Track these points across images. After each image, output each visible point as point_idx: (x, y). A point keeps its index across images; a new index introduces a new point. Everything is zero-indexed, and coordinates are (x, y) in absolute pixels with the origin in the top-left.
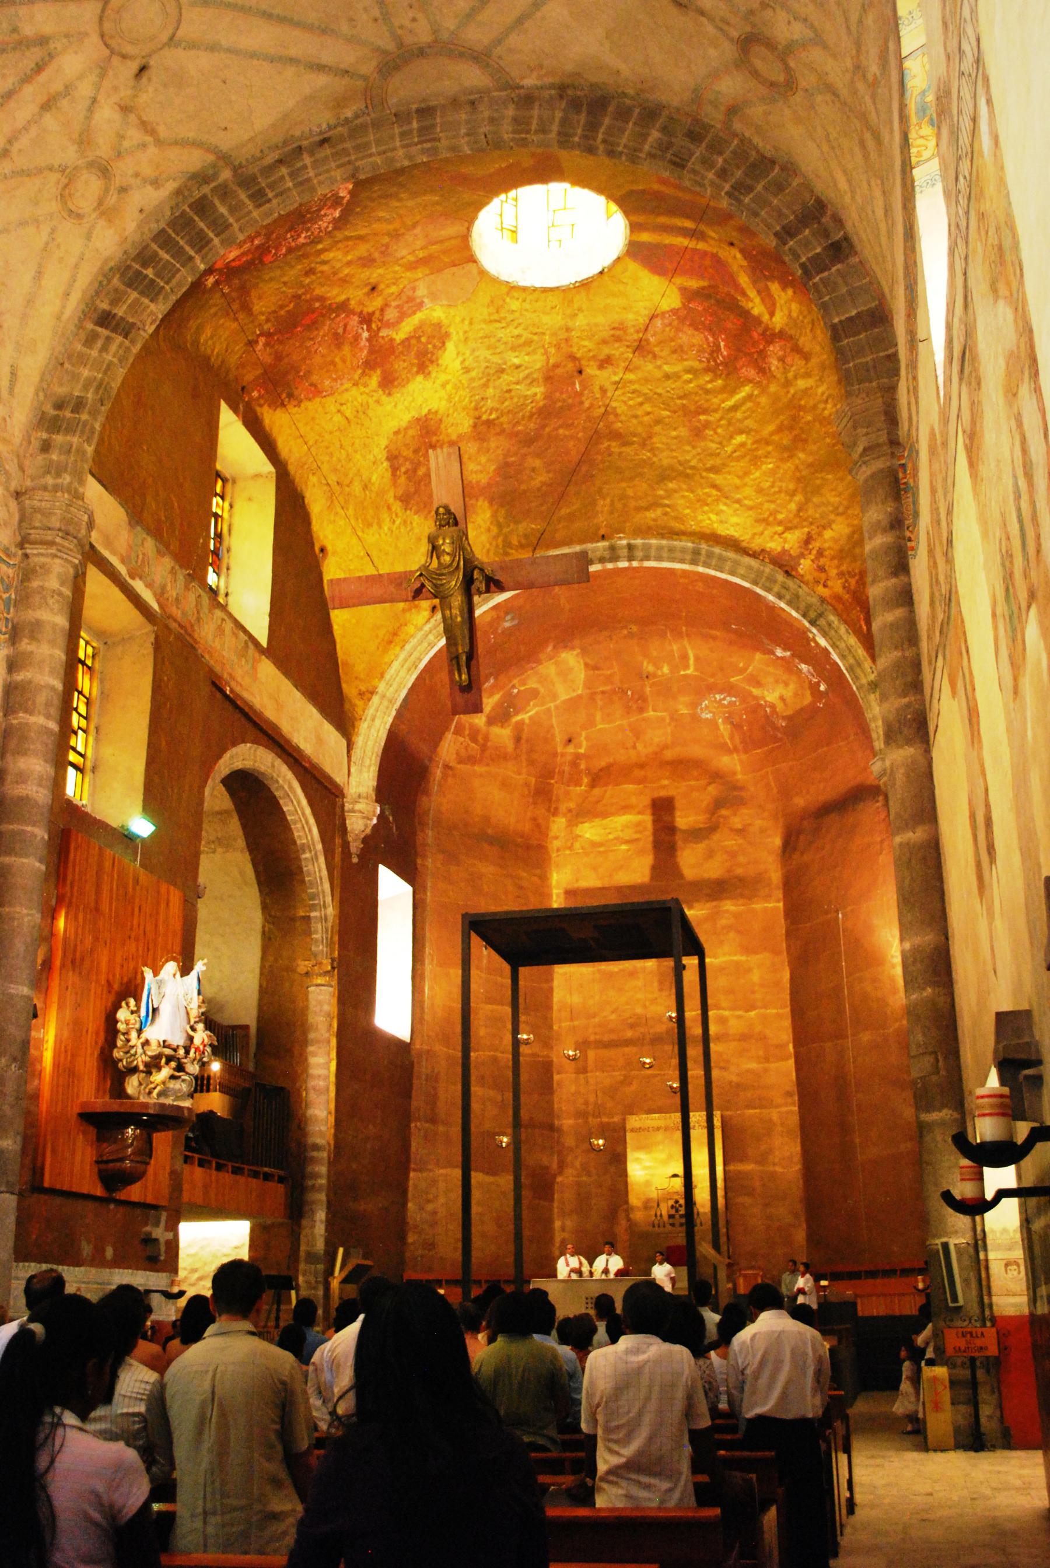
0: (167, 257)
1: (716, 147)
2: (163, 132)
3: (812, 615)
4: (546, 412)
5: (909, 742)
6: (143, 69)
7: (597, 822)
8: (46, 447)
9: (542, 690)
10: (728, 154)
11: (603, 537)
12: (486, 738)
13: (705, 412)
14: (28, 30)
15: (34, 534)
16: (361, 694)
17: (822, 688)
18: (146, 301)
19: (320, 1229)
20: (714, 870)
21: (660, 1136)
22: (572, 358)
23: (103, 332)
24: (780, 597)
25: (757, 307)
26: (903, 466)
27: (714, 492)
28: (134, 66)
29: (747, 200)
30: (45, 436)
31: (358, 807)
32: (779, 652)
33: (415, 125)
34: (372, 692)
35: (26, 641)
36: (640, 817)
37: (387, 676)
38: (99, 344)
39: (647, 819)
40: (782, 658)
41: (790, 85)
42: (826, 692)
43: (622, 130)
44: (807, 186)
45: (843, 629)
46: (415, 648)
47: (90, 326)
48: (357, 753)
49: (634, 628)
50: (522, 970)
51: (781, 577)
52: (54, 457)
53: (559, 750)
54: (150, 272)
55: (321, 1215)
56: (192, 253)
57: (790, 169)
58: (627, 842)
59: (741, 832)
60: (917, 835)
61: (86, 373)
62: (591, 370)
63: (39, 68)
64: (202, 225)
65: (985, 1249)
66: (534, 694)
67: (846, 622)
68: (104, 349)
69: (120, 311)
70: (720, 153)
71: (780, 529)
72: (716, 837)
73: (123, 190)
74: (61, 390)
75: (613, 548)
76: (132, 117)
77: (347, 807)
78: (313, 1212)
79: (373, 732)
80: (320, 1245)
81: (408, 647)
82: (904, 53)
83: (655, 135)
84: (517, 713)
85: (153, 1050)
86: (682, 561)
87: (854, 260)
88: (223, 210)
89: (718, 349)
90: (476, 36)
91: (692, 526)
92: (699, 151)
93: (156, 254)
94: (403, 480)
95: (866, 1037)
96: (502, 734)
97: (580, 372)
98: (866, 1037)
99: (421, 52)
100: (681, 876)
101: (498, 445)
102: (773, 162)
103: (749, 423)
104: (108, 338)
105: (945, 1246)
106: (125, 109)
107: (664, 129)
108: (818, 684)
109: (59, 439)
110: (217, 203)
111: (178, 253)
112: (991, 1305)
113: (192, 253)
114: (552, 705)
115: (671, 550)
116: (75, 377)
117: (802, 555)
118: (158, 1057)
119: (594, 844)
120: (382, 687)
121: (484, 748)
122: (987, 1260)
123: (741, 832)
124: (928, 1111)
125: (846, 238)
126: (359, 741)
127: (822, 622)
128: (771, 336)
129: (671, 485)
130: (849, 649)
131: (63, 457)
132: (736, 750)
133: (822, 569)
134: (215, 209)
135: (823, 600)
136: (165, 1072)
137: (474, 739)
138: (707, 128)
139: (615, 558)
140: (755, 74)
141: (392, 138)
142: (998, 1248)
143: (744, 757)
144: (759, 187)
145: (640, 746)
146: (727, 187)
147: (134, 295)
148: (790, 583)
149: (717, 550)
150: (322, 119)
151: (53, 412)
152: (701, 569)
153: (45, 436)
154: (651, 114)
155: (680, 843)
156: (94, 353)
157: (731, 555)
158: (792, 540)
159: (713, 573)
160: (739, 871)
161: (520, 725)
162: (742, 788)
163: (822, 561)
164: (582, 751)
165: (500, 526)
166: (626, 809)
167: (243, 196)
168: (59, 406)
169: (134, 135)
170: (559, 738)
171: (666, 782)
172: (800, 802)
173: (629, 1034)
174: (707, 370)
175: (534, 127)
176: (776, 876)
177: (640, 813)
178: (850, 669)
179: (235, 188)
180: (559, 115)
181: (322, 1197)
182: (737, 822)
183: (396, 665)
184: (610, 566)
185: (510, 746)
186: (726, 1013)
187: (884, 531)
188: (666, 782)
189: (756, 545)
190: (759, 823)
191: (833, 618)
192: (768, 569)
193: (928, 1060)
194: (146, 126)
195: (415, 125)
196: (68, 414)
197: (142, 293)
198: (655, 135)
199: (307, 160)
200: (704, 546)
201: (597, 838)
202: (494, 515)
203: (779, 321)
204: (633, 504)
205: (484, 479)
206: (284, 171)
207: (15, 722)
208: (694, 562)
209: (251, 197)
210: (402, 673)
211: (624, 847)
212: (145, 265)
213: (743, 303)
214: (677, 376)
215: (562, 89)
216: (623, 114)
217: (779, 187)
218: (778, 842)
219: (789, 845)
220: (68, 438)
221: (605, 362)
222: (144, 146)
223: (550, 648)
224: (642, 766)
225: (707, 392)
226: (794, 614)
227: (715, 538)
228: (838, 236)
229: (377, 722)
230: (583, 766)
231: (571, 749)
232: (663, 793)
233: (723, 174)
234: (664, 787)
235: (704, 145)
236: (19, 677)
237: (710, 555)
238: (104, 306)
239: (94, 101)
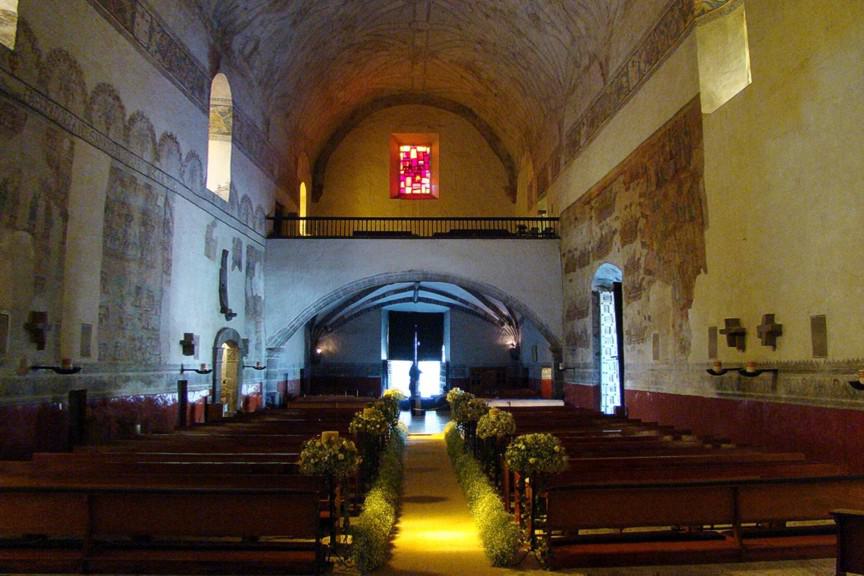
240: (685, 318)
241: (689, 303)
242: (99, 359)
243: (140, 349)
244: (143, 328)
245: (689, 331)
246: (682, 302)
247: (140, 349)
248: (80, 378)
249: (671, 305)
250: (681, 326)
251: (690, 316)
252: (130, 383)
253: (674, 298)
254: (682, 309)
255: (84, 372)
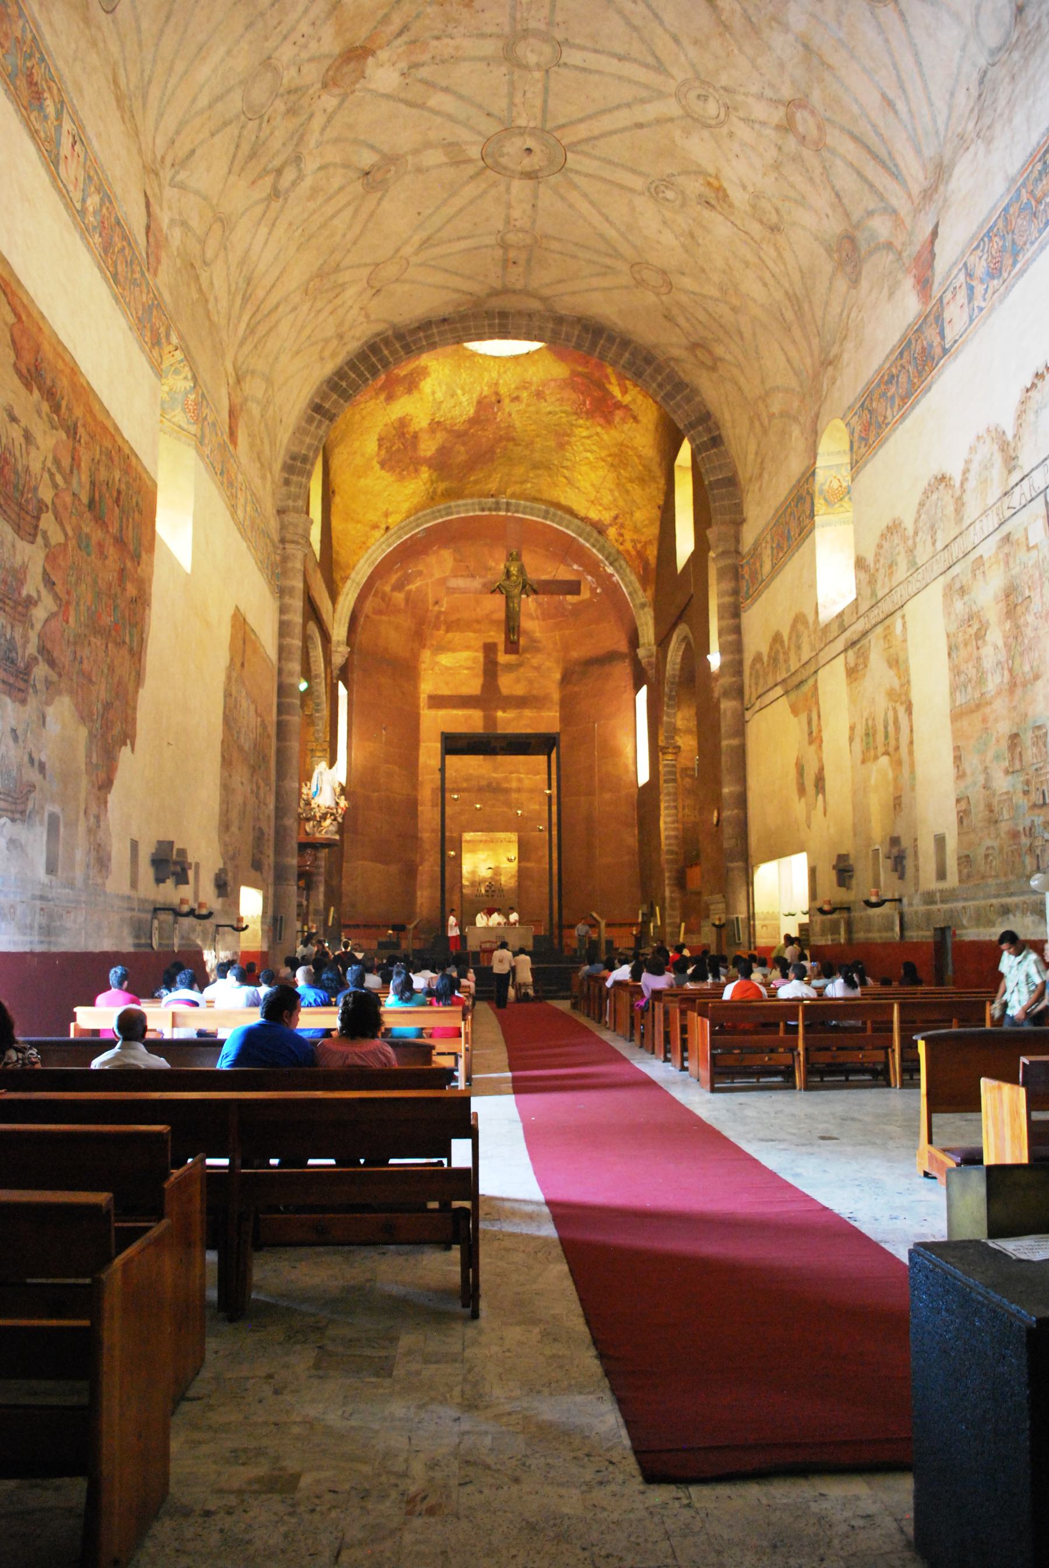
0: (353, 376)
1: (658, 370)
2: (373, 317)
3: (611, 559)
4: (474, 421)
5: (734, 699)
6: (378, 291)
7: (450, 654)
8: (287, 482)
9: (425, 571)
10: (664, 374)
11: (492, 496)
12: (390, 599)
13: (569, 435)
14: (340, 281)
15: (289, 536)
16: (342, 578)
17: (598, 591)
18: (342, 401)
19: (321, 897)
20: (519, 690)
21: (481, 845)
22: (497, 394)
23: (318, 417)
24: (594, 546)
25: (616, 391)
26: (742, 566)
27: (564, 480)
28: (374, 291)
29: (672, 403)
30: (286, 476)
31: (339, 649)
32: (575, 567)
33: (497, 321)
34: (347, 578)
35: (287, 598)
36: (476, 654)
37: (357, 568)
38: (315, 424)
39: (480, 656)
40: (577, 570)
41: (714, 369)
42: (599, 594)
43: (610, 348)
44: (702, 403)
45: (628, 570)
46: (374, 552)
47: (309, 411)
48: (337, 615)
49: (489, 541)
50: (448, 757)
51: (595, 534)
52: (292, 489)
53: (430, 608)
54: (344, 384)
55: (322, 889)
56: (368, 376)
57: (695, 391)
58: (467, 668)
59: (537, 669)
60: (735, 742)
61: (308, 440)
62: (506, 401)
63: (337, 296)
64: (374, 359)
65: (754, 920)
66: (420, 573)
67: (630, 566)
68: (318, 427)
69: (327, 405)
70: (660, 374)
71: (601, 508)
72: (522, 670)
73: (345, 344)
74: (295, 449)
75: (497, 503)
76: (363, 312)
77: (333, 649)
78: (318, 888)
79: (347, 603)
80: (322, 905)
81: (370, 551)
82: (818, 465)
83: (627, 355)
84: (408, 584)
85: (323, 810)
86: (538, 516)
87: (723, 448)
88: (386, 352)
89: (584, 404)
90: (547, 292)
91: (546, 496)
92: (649, 370)
93: (346, 373)
94: (383, 452)
95: (607, 796)
96: (399, 597)
97: (499, 402)
98: (607, 796)
99: (514, 292)
100: (499, 692)
101: (440, 437)
102: (687, 386)
103: (594, 448)
104: (320, 421)
105: (737, 918)
106: (362, 309)
107: (632, 354)
108: (596, 589)
109: (294, 478)
110: (383, 347)
111: (360, 375)
112: (754, 942)
113: (368, 376)
114: (430, 581)
115: (532, 509)
116: (302, 442)
117: (611, 525)
118: (326, 813)
119: (447, 668)
120: (353, 575)
121: (388, 605)
122: (754, 925)
123: (537, 669)
124: (731, 862)
125: (720, 436)
126: (339, 607)
127: (617, 564)
128: (618, 406)
129: (539, 472)
130: (631, 582)
131: (297, 490)
132: (538, 618)
133: (621, 535)
134: (381, 351)
135: (619, 552)
136: (328, 822)
137: (383, 599)
138: (654, 358)
139: (498, 509)
140: (696, 356)
141: (483, 326)
142: (760, 919)
143: (541, 623)
144: (679, 398)
145: (478, 610)
146: (662, 394)
147: (335, 396)
148: (600, 538)
149: (559, 513)
150: (447, 311)
151: (289, 462)
152: (548, 522)
153: (286, 476)
154: (626, 343)
155: (499, 672)
156: (313, 429)
157: (568, 517)
158: (606, 517)
159: (555, 525)
160: (535, 692)
161: (409, 592)
162: (539, 642)
163: (622, 531)
164: (443, 609)
165: (432, 482)
166: (468, 648)
167: (398, 346)
168: (294, 458)
169: (362, 319)
170: (431, 600)
171: (493, 633)
172: (574, 655)
173: (465, 785)
174: (576, 413)
175: (563, 337)
176: (556, 696)
177: (476, 651)
178: (630, 594)
179: (394, 340)
180: (576, 332)
181: (322, 879)
182: (535, 662)
183: (362, 561)
184: (494, 513)
185: (403, 605)
186: (522, 776)
187: (730, 595)
188: (493, 633)
189: (582, 513)
190: (548, 664)
191: (623, 562)
192: (589, 528)
193: (733, 841)
194: (367, 316)
195: (497, 321)
196: (299, 464)
197: (339, 396)
198: (627, 355)
199: (435, 330)
200: (552, 510)
201: (449, 665)
202: (430, 476)
203: (627, 399)
204: (513, 479)
205: (429, 454)
206: (421, 334)
207: (285, 643)
208: (545, 518)
209: (403, 347)
210: (366, 566)
211: (465, 672)
212: (341, 378)
213: (607, 386)
214: (555, 413)
215: (579, 320)
216: (611, 339)
217: (688, 400)
218: (558, 676)
219: (566, 679)
220: (300, 478)
221: (516, 399)
222: (362, 323)
223: (435, 548)
224: (478, 622)
225: (572, 425)
226: (600, 557)
227: (558, 506)
228: (716, 434)
229: (350, 597)
230: (442, 619)
231: (436, 608)
232: (490, 640)
233: (661, 386)
234: (491, 636)
235: (652, 367)
236: (285, 617)
237: (554, 515)
238: (317, 400)
239: (351, 307)
240: (103, 807)
241: (106, 785)
242: (960, 881)
243: (1031, 849)
244: (1035, 806)
245: (108, 834)
246: (102, 775)
247: (1031, 849)
248: (939, 910)
249: (83, 767)
250: (98, 818)
251: (109, 805)
252: (1011, 916)
253: (89, 756)
254: (100, 788)
255: (942, 902)
